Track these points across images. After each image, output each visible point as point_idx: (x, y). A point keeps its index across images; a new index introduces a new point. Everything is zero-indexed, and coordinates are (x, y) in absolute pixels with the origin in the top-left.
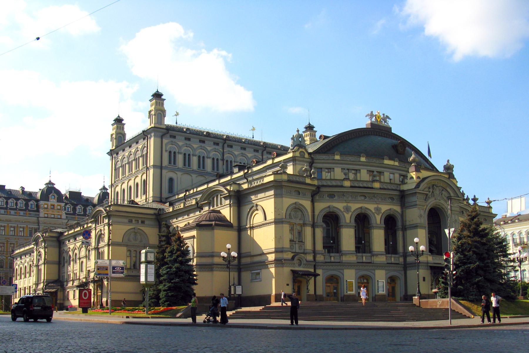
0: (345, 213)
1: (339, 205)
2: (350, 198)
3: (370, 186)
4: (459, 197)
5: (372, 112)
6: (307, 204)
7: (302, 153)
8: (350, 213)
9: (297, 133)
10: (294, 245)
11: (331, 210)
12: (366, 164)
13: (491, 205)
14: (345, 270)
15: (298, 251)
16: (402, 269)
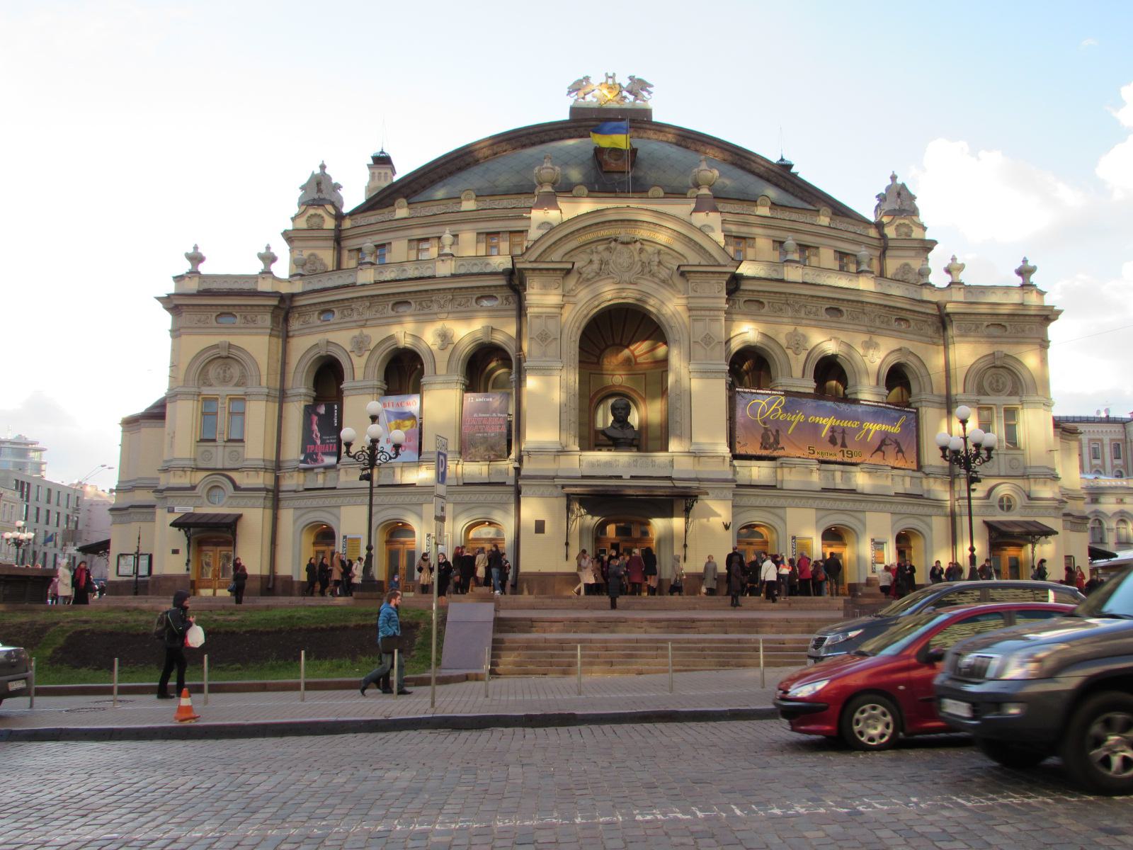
0: (352, 356)
2: (367, 315)
4: (719, 265)
6: (257, 345)
7: (315, 220)
8: (367, 353)
9: (318, 171)
10: (213, 450)
11: (323, 353)
12: (475, 215)
13: (1033, 279)
14: (342, 508)
15: (220, 466)
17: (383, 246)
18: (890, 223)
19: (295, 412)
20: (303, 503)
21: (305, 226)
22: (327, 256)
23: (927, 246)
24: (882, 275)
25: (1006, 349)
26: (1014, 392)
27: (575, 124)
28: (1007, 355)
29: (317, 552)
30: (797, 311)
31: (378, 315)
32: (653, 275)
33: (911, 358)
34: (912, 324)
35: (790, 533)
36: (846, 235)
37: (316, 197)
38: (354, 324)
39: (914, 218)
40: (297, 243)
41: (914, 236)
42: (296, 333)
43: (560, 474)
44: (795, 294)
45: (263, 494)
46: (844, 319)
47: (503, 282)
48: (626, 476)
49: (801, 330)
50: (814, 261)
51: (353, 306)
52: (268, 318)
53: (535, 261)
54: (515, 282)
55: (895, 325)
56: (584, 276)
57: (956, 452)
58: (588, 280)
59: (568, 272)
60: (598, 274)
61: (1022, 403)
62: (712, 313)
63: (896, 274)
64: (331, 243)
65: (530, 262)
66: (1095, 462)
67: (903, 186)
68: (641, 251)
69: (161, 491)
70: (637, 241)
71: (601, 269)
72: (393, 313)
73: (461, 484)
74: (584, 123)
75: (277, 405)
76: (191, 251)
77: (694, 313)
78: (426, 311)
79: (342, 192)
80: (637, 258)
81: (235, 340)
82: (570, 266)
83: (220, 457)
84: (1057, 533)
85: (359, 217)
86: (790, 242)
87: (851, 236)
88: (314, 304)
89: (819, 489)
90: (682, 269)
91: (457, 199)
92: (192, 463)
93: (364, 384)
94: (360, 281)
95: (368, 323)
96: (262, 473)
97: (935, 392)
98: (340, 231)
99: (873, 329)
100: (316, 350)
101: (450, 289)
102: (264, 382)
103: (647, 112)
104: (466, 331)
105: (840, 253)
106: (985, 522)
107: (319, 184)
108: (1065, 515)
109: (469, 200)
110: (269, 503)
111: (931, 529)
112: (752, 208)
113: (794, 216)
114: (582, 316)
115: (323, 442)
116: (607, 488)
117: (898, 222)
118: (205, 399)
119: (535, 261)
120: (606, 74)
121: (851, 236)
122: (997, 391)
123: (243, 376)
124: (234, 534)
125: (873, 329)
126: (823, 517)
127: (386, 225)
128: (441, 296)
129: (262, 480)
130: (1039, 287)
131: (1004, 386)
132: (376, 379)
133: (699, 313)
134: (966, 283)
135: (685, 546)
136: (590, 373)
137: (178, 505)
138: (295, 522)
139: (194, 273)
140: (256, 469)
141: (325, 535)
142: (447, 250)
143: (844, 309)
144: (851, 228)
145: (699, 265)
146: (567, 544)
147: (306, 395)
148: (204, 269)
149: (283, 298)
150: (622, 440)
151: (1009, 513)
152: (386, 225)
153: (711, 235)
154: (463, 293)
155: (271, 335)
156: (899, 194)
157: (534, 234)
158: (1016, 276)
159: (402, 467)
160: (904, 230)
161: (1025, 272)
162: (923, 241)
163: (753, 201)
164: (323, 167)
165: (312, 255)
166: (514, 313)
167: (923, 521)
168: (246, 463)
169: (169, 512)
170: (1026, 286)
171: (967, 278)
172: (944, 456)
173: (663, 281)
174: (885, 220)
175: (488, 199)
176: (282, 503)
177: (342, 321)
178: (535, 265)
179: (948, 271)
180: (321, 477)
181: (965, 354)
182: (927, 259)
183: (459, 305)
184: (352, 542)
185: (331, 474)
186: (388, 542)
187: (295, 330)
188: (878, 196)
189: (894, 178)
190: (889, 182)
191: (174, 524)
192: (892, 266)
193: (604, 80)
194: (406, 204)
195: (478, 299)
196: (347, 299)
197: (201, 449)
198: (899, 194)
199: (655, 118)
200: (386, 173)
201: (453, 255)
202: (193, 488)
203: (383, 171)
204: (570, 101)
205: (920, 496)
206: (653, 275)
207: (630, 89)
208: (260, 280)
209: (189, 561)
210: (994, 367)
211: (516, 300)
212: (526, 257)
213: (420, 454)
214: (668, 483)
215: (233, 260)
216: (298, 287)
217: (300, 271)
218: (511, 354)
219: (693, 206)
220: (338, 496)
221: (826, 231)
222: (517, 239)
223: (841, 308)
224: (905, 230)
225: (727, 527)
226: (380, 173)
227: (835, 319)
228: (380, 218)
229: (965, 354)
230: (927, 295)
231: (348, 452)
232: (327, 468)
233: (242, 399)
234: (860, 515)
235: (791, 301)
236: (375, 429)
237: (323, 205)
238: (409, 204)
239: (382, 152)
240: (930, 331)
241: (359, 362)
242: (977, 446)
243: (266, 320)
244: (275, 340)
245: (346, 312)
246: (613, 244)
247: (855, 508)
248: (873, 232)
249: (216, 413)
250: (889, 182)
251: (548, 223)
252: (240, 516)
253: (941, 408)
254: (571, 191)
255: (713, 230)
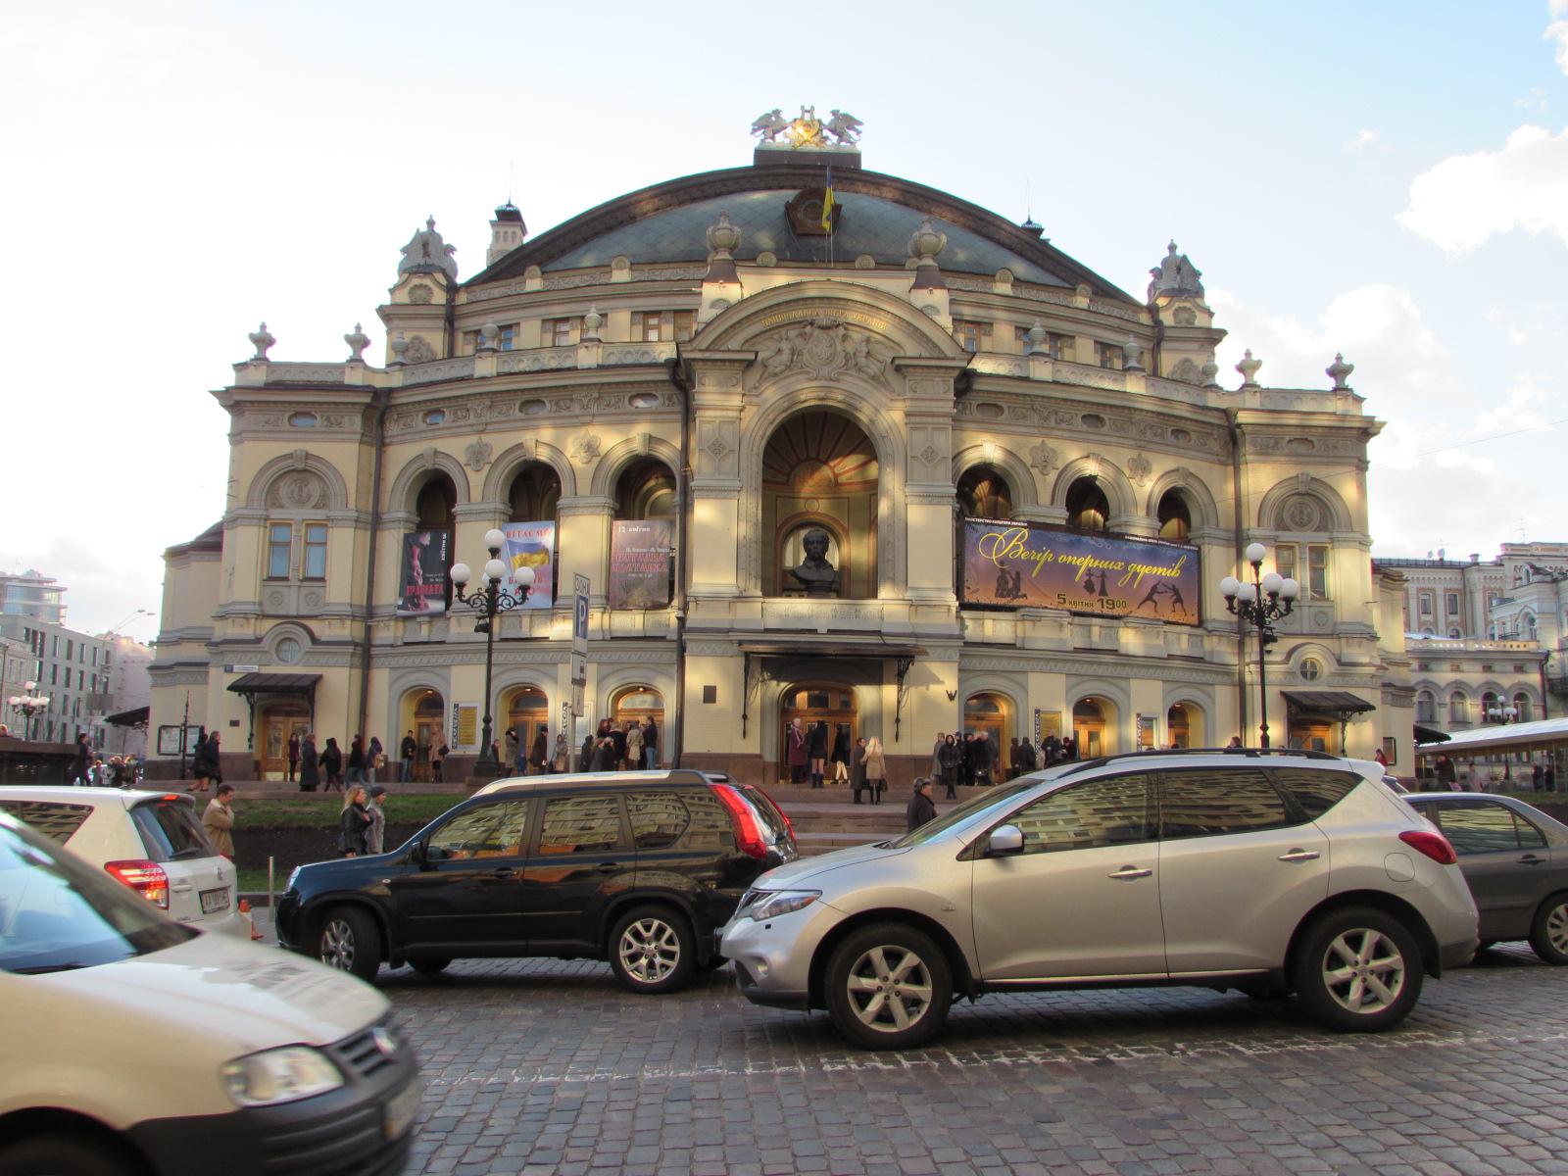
0: (468, 470)
1: (452, 447)
2: (488, 417)
3: (568, 364)
4: (946, 358)
5: (777, 113)
7: (421, 292)
8: (488, 467)
9: (424, 228)
11: (429, 466)
14: (454, 670)
15: (293, 612)
16: (674, 657)
17: (509, 327)
18: (1167, 307)
19: (392, 543)
20: (401, 661)
21: (407, 300)
22: (436, 341)
23: (1214, 337)
24: (1155, 373)
25: (1314, 471)
26: (1322, 527)
27: (762, 172)
28: (1314, 480)
29: (421, 726)
30: (1046, 419)
31: (502, 418)
32: (860, 370)
33: (1191, 481)
34: (1194, 436)
35: (1033, 704)
36: (1110, 321)
37: (422, 262)
38: (470, 429)
39: (1198, 300)
40: (396, 323)
41: (1197, 323)
42: (395, 440)
43: (736, 626)
44: (1043, 397)
45: (350, 649)
46: (1105, 430)
47: (666, 377)
48: (823, 629)
49: (1051, 443)
50: (1068, 354)
51: (469, 406)
52: (358, 420)
53: (707, 350)
54: (680, 378)
55: (1171, 440)
56: (770, 369)
57: (1246, 603)
58: (776, 375)
59: (749, 364)
60: (788, 367)
61: (1332, 540)
62: (936, 420)
63: (1173, 373)
64: (441, 323)
65: (700, 351)
66: (1425, 618)
67: (1184, 259)
68: (845, 338)
69: (216, 644)
70: (838, 326)
71: (792, 361)
72: (522, 416)
73: (608, 637)
74: (771, 172)
75: (369, 533)
76: (256, 331)
77: (913, 419)
78: (565, 413)
79: (455, 257)
80: (839, 348)
81: (314, 448)
82: (751, 356)
83: (293, 601)
84: (1372, 708)
85: (478, 289)
86: (1038, 328)
87: (1118, 322)
88: (419, 402)
89: (1070, 648)
90: (897, 362)
91: (605, 267)
92: (257, 608)
93: (482, 506)
94: (478, 373)
95: (490, 427)
96: (348, 622)
97: (1222, 525)
98: (454, 307)
99: (1143, 444)
100: (421, 463)
101: (595, 384)
102: (352, 504)
103: (856, 158)
104: (617, 442)
105: (1102, 344)
106: (1282, 693)
107: (425, 245)
108: (1385, 685)
109: (621, 269)
110: (357, 661)
111: (1214, 702)
112: (989, 285)
113: (1043, 296)
114: (766, 423)
115: (426, 580)
116: (797, 646)
117: (1176, 306)
118: (273, 525)
119: (707, 350)
120: (802, 107)
121: (1118, 322)
122: (1302, 526)
123: (324, 495)
124: (312, 700)
125: (1143, 444)
126: (1078, 684)
127: (513, 301)
128: (585, 393)
129: (346, 631)
130: (1356, 392)
131: (1310, 519)
132: (498, 500)
133: (918, 419)
134: (1264, 386)
135: (898, 720)
136: (777, 497)
137: (238, 663)
138: (391, 685)
139: (261, 360)
140: (341, 617)
141: (430, 703)
142: (592, 334)
143: (1106, 417)
144: (1116, 312)
145: (920, 358)
146: (745, 717)
147: (406, 521)
148: (274, 354)
149: (377, 393)
150: (817, 584)
151: (1314, 682)
152: (513, 301)
153: (936, 318)
154: (611, 391)
155: (361, 442)
156: (1179, 269)
157: (706, 314)
158: (1328, 377)
159: (531, 616)
160: (1185, 315)
161: (1339, 371)
162: (1209, 330)
163: (990, 276)
164: (431, 223)
165: (416, 338)
166: (679, 417)
167: (1204, 692)
168: (327, 608)
169: (226, 671)
170: (1341, 391)
171: (1263, 378)
172: (1231, 608)
173: (873, 378)
174: (1162, 302)
175: (646, 268)
176: (376, 662)
177: (454, 424)
178: (707, 355)
179: (1241, 369)
180: (425, 629)
181: (1261, 479)
182: (1213, 354)
183: (608, 405)
184: (465, 714)
185: (439, 624)
186: (512, 713)
187: (394, 436)
188: (1152, 271)
189: (1172, 248)
190: (1167, 254)
191: (232, 688)
192: (1169, 361)
193: (798, 115)
194: (539, 273)
195: (632, 398)
196: (461, 396)
197: (269, 590)
198: (1179, 269)
199: (867, 165)
200: (514, 233)
201: (599, 341)
202: (258, 640)
203: (510, 230)
204: (755, 141)
205: (1200, 660)
206: (860, 370)
207: (833, 127)
208: (347, 370)
209: (252, 735)
210: (1298, 494)
211: (682, 399)
212: (694, 344)
213: (554, 598)
214: (875, 640)
215: (312, 343)
216: (397, 380)
217: (400, 359)
218: (674, 469)
219: (913, 280)
220: (450, 652)
221: (1083, 316)
222: (683, 321)
223: (1102, 415)
224: (1186, 315)
225: (951, 697)
226: (506, 233)
227: (1095, 430)
228: (505, 291)
229: (1261, 479)
230: (1212, 400)
231: (460, 595)
232: (434, 616)
233: (323, 525)
234: (1122, 683)
235: (1037, 406)
236: (495, 566)
237: (430, 274)
238: (543, 273)
239: (509, 205)
240: (1216, 447)
241: (477, 479)
242: (1273, 595)
243: (357, 422)
244: (366, 448)
245: (459, 413)
246: (808, 329)
247: (1115, 674)
248: (1145, 318)
249: (288, 544)
250: (1167, 254)
251: (724, 300)
252: (320, 677)
253: (1228, 547)
254: (754, 259)
255: (938, 312)
